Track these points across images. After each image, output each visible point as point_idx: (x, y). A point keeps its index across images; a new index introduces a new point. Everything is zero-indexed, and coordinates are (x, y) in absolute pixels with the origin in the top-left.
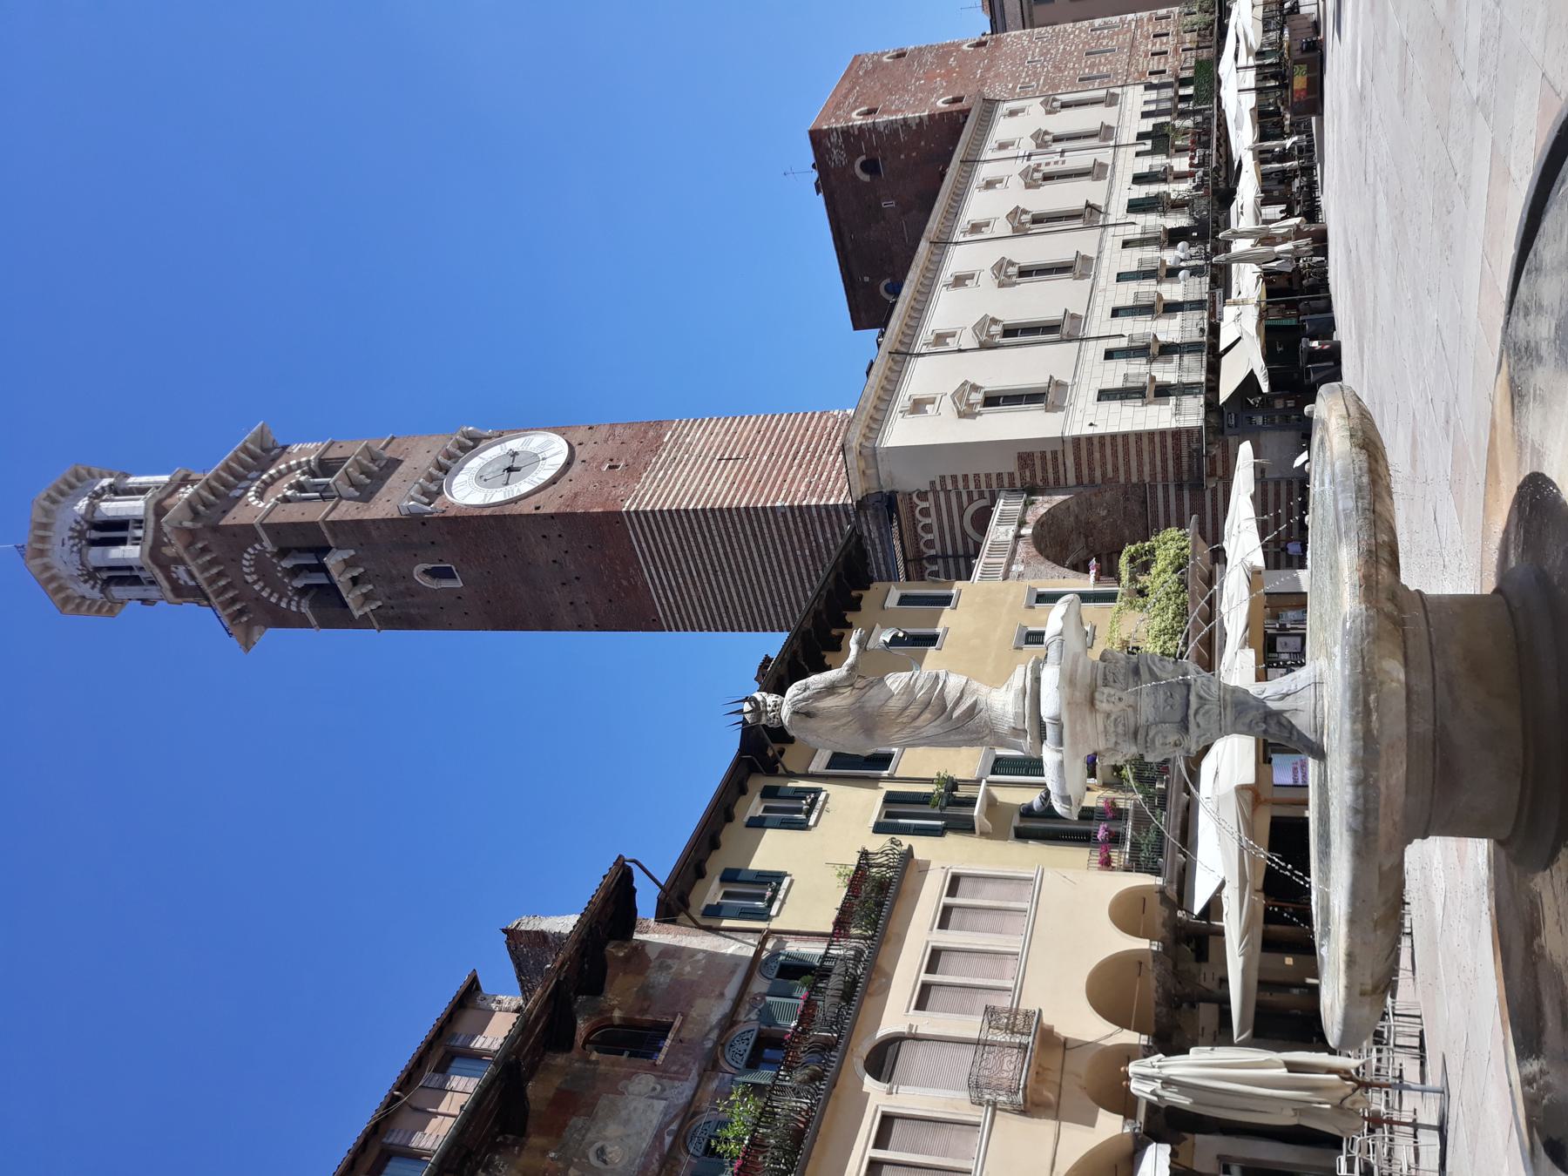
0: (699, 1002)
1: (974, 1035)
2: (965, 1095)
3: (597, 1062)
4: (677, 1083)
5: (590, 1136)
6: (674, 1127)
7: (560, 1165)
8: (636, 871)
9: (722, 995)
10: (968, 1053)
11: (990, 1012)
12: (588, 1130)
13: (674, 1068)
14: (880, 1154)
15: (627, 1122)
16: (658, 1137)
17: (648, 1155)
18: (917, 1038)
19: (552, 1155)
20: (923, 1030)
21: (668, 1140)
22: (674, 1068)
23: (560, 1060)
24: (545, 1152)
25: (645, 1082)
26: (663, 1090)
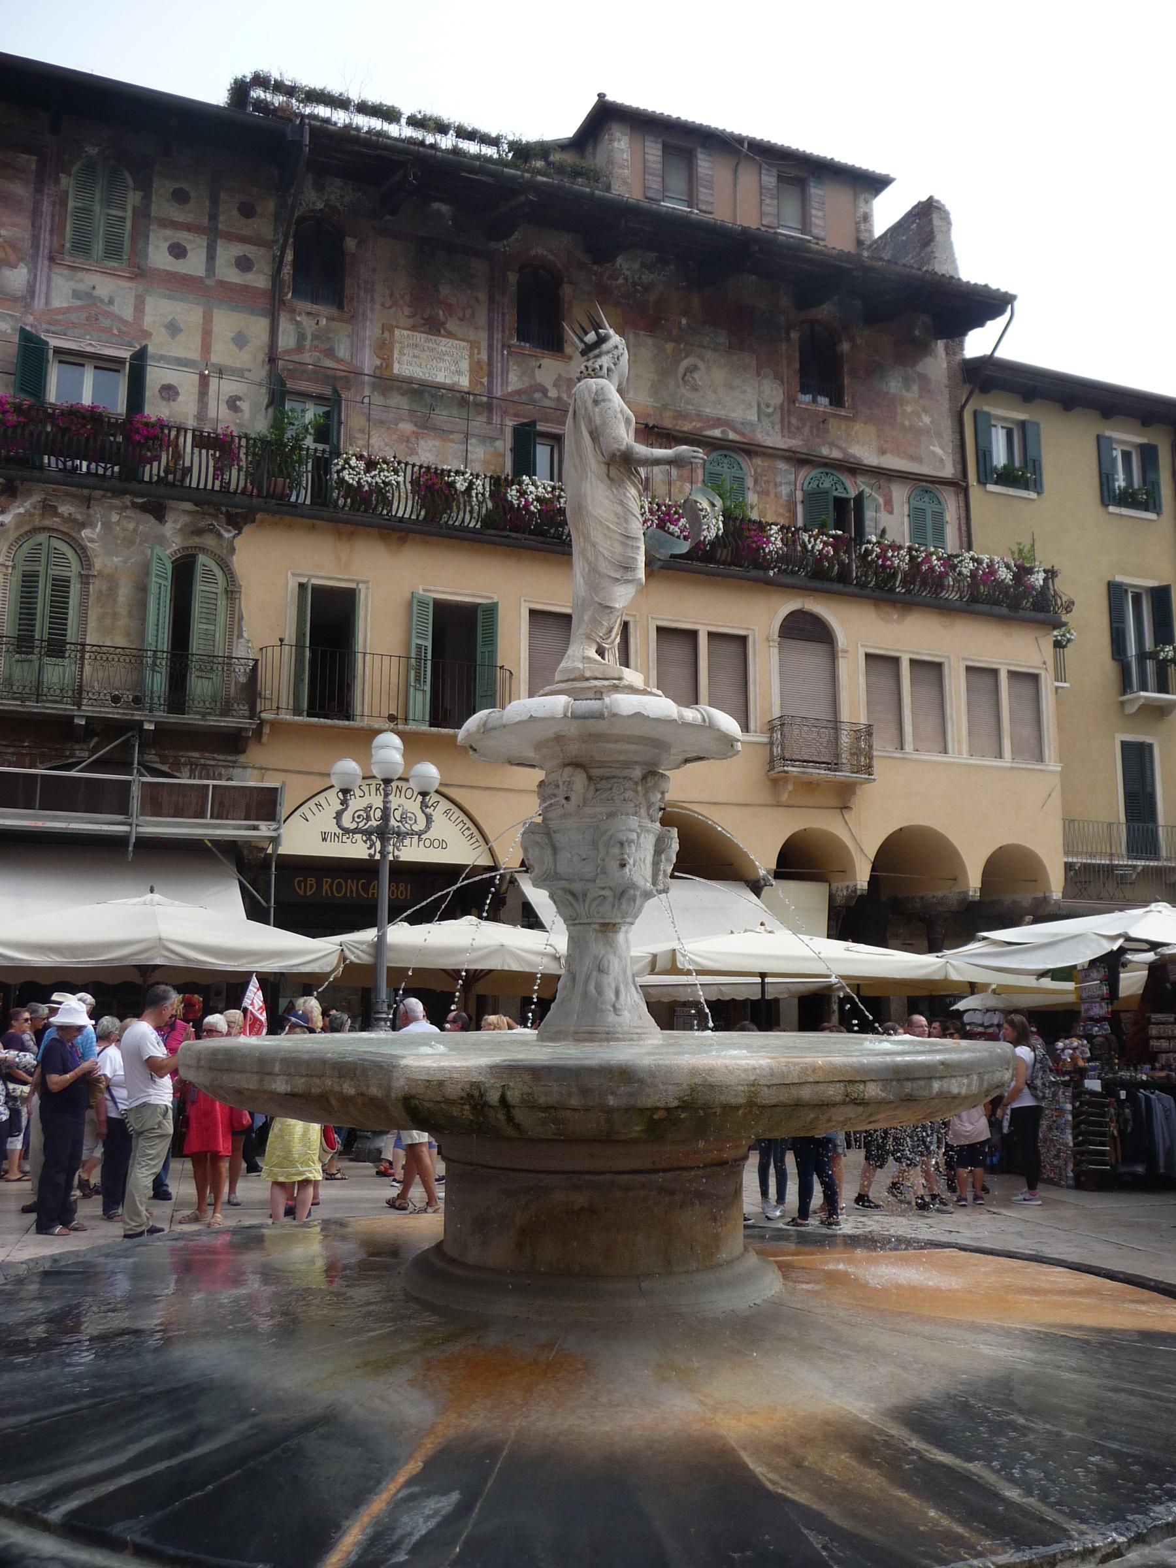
0: (872, 430)
1: (845, 716)
2: (777, 713)
3: (788, 339)
4: (778, 427)
5: (709, 354)
6: (732, 436)
7: (674, 333)
8: (1002, 320)
9: (883, 452)
10: (824, 714)
11: (869, 731)
12: (715, 350)
13: (794, 421)
14: (703, 641)
15: (730, 387)
16: (719, 422)
17: (699, 416)
18: (833, 655)
19: (684, 321)
20: (843, 666)
21: (717, 433)
22: (794, 421)
23: (785, 301)
24: (685, 314)
25: (773, 393)
26: (769, 415)
